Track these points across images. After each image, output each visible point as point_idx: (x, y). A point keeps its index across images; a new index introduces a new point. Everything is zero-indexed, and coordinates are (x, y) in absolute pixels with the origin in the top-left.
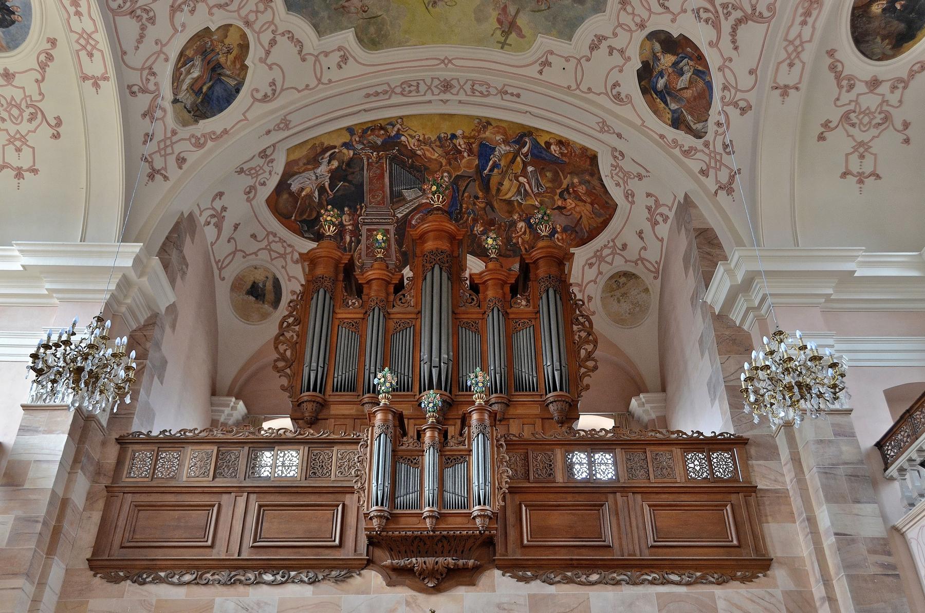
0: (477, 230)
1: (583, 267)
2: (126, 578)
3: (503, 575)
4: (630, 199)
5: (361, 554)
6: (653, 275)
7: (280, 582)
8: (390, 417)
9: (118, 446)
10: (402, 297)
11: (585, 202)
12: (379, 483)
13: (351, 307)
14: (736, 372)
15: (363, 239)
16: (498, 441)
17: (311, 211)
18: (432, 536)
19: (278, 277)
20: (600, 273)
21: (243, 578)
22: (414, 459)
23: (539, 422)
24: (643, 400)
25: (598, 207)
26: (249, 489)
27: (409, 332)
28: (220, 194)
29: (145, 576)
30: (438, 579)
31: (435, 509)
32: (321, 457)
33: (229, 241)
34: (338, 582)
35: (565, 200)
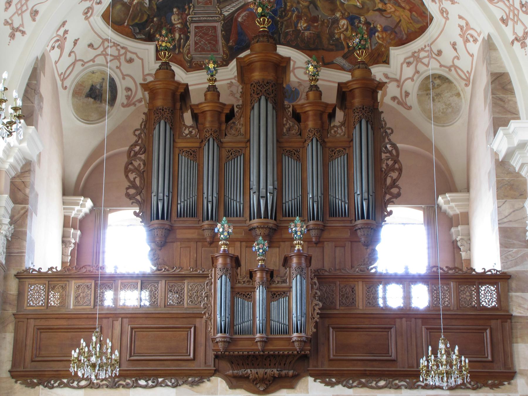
0: (301, 26)
1: (402, 64)
2: (38, 384)
3: (315, 381)
4: (445, 15)
5: (210, 366)
6: (464, 82)
7: (152, 386)
8: (228, 260)
9: (17, 280)
10: (232, 125)
11: (404, 8)
12: (222, 315)
13: (188, 136)
14: (509, 215)
15: (192, 36)
16: (312, 279)
17: (142, 15)
18: (263, 355)
19: (113, 77)
20: (417, 72)
21: (124, 383)
22: (248, 295)
23: (348, 244)
24: (449, 198)
25: (416, 15)
26: (123, 315)
27: (240, 160)
28: (64, 24)
29: (52, 382)
30: (266, 384)
31: (264, 335)
32: (176, 289)
33: (70, 55)
34: (194, 386)
35: (385, 4)
